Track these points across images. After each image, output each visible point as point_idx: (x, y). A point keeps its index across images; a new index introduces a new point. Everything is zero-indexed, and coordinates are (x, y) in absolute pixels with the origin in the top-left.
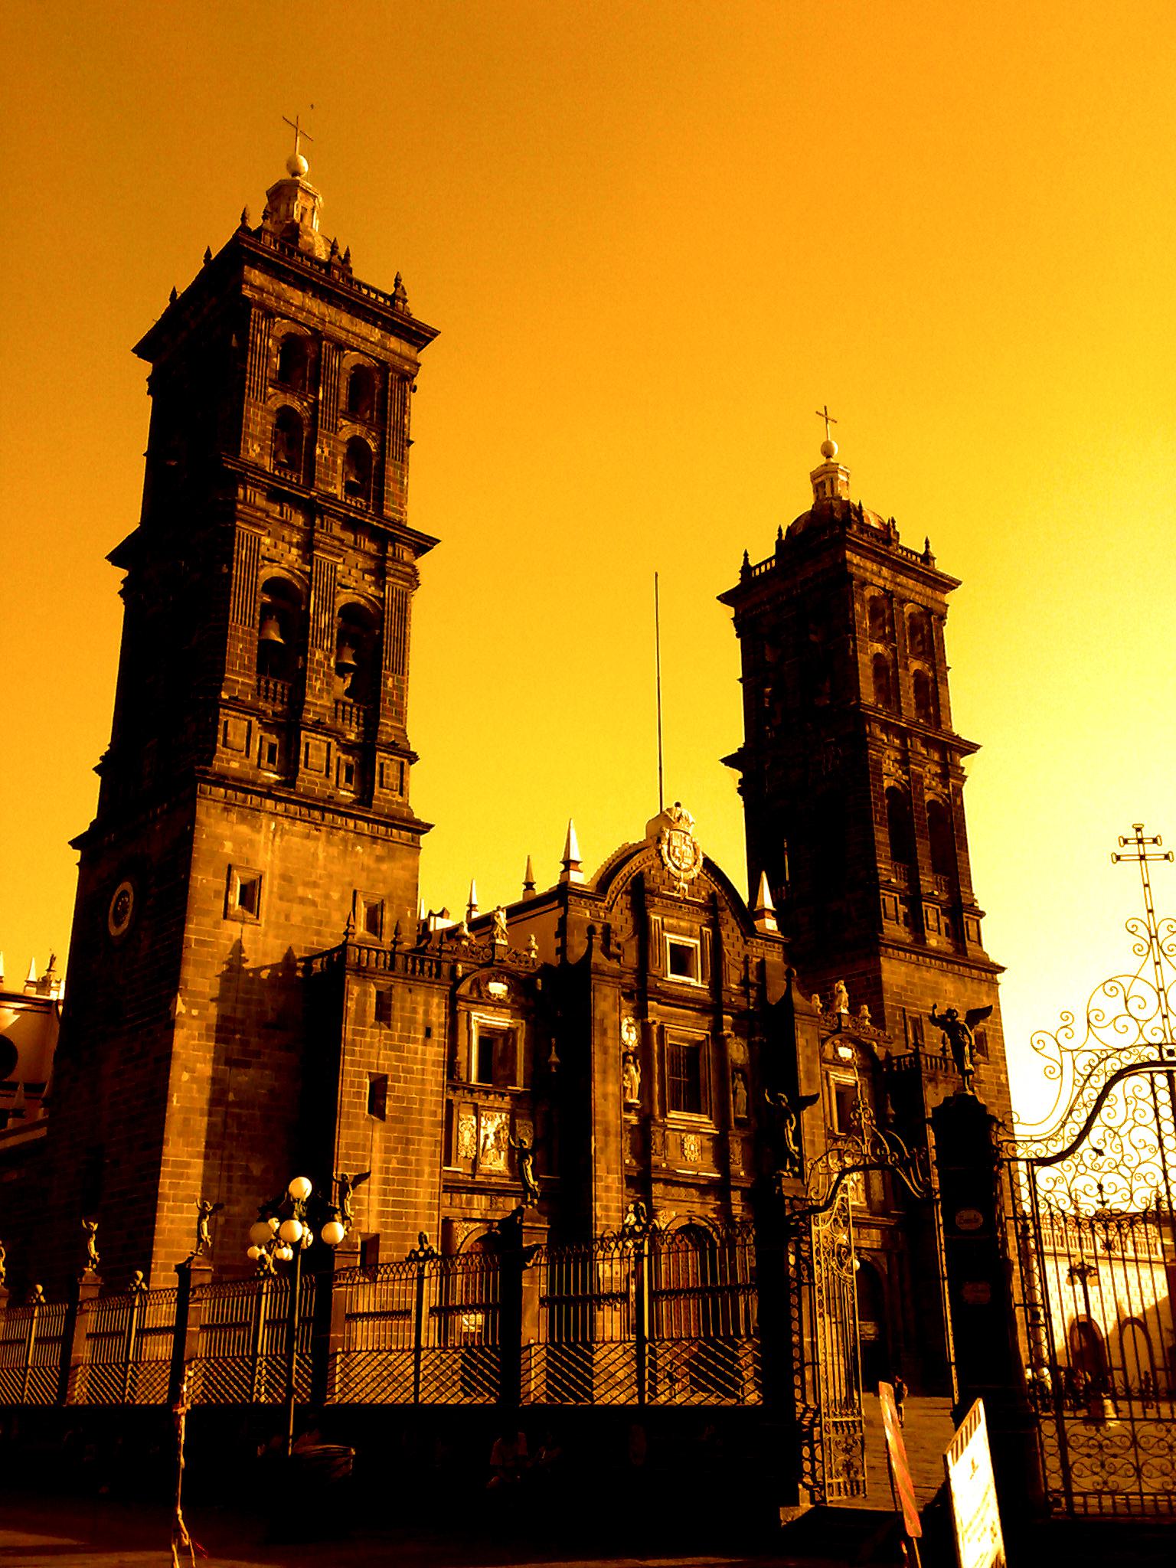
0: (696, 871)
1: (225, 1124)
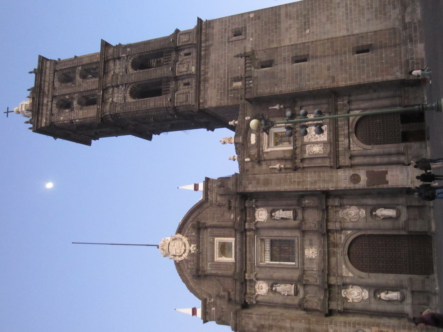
0: (185, 240)
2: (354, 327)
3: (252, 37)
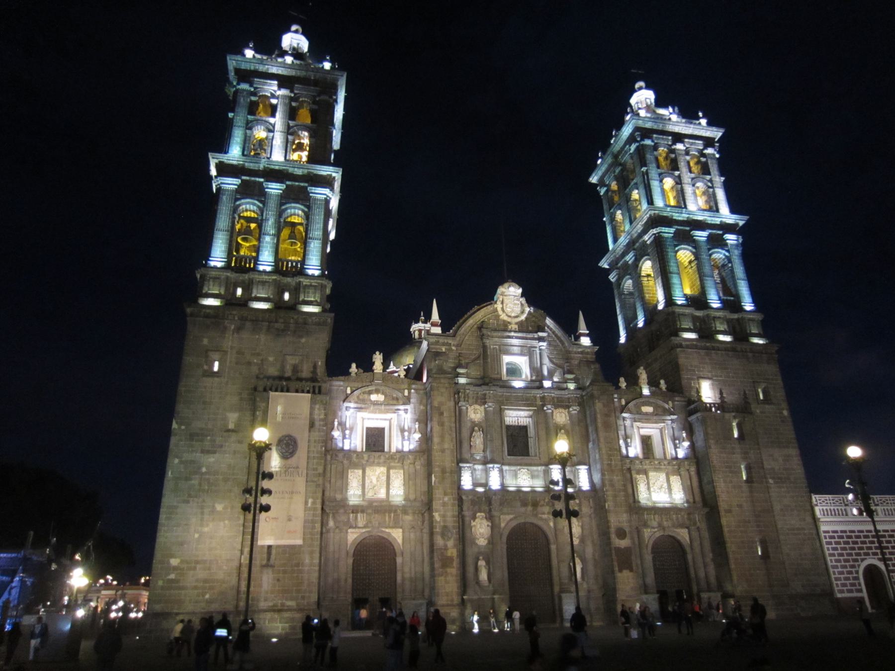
0: (523, 317)
1: (200, 484)
2: (454, 527)
3: (761, 412)
